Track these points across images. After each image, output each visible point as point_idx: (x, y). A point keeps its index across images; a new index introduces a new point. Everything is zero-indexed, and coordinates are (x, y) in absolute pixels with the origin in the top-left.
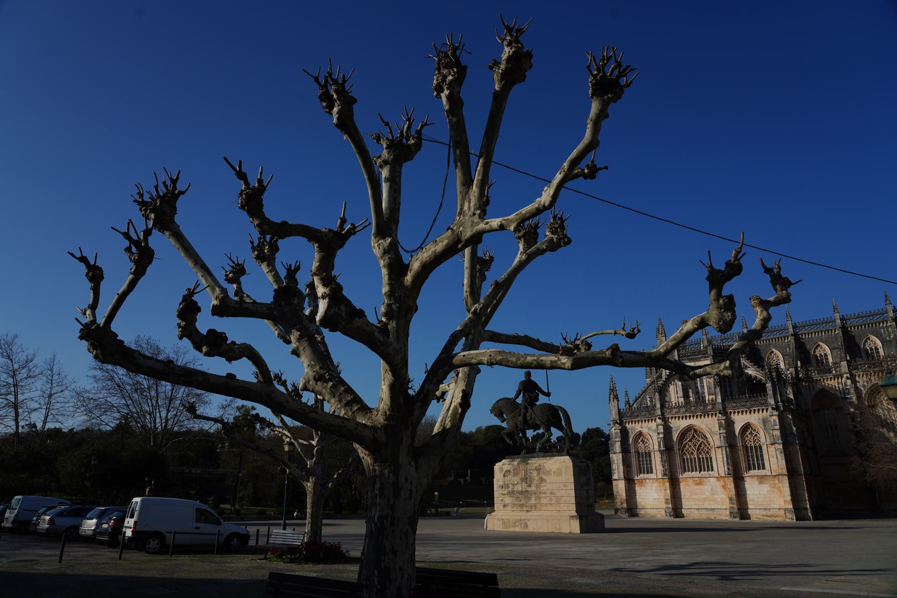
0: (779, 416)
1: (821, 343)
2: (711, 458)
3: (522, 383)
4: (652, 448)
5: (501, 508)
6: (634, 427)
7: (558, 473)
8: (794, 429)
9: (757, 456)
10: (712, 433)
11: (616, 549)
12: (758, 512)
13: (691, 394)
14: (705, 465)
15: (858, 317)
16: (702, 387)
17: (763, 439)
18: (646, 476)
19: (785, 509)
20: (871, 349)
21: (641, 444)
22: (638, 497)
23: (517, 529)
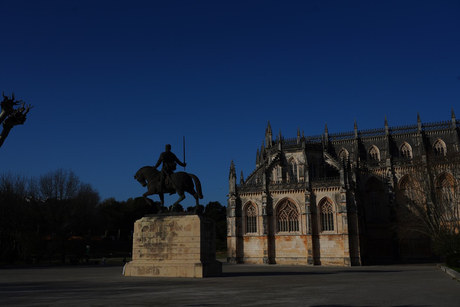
0: (346, 193)
1: (374, 146)
2: (298, 222)
3: (163, 154)
4: (257, 214)
5: (138, 257)
6: (246, 198)
7: (188, 228)
8: (356, 202)
9: (329, 221)
10: (300, 204)
11: (235, 292)
12: (326, 260)
13: (287, 176)
14: (294, 226)
15: (399, 130)
17: (334, 209)
18: (251, 234)
19: (345, 258)
20: (405, 152)
21: (249, 211)
23: (151, 275)
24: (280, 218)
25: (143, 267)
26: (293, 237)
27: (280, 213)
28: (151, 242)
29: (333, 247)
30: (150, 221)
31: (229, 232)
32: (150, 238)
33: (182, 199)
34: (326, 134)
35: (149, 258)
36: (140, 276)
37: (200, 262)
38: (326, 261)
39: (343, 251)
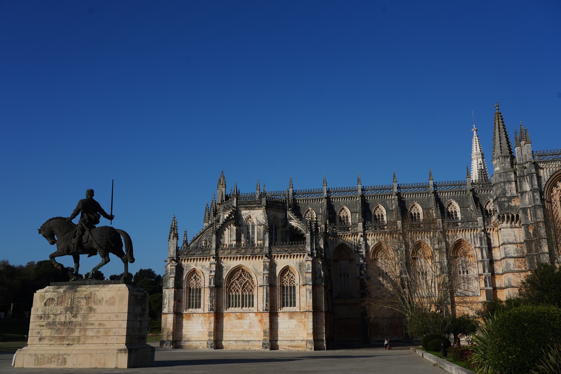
0: (312, 261)
1: (345, 207)
2: (253, 296)
3: (83, 202)
4: (202, 285)
6: (189, 265)
7: (111, 302)
8: (322, 273)
10: (257, 274)
12: (285, 343)
13: (243, 239)
14: (247, 301)
16: (253, 233)
17: (297, 281)
18: (194, 310)
19: (307, 341)
20: (379, 216)
22: (184, 330)
23: (53, 366)
24: (231, 291)
25: (43, 355)
26: (245, 314)
27: (232, 284)
28: (57, 320)
29: (293, 326)
30: (57, 292)
31: (165, 307)
32: (55, 315)
33: (106, 263)
34: (291, 190)
35: (52, 343)
36: (38, 367)
37: (125, 347)
38: (285, 344)
39: (306, 332)
